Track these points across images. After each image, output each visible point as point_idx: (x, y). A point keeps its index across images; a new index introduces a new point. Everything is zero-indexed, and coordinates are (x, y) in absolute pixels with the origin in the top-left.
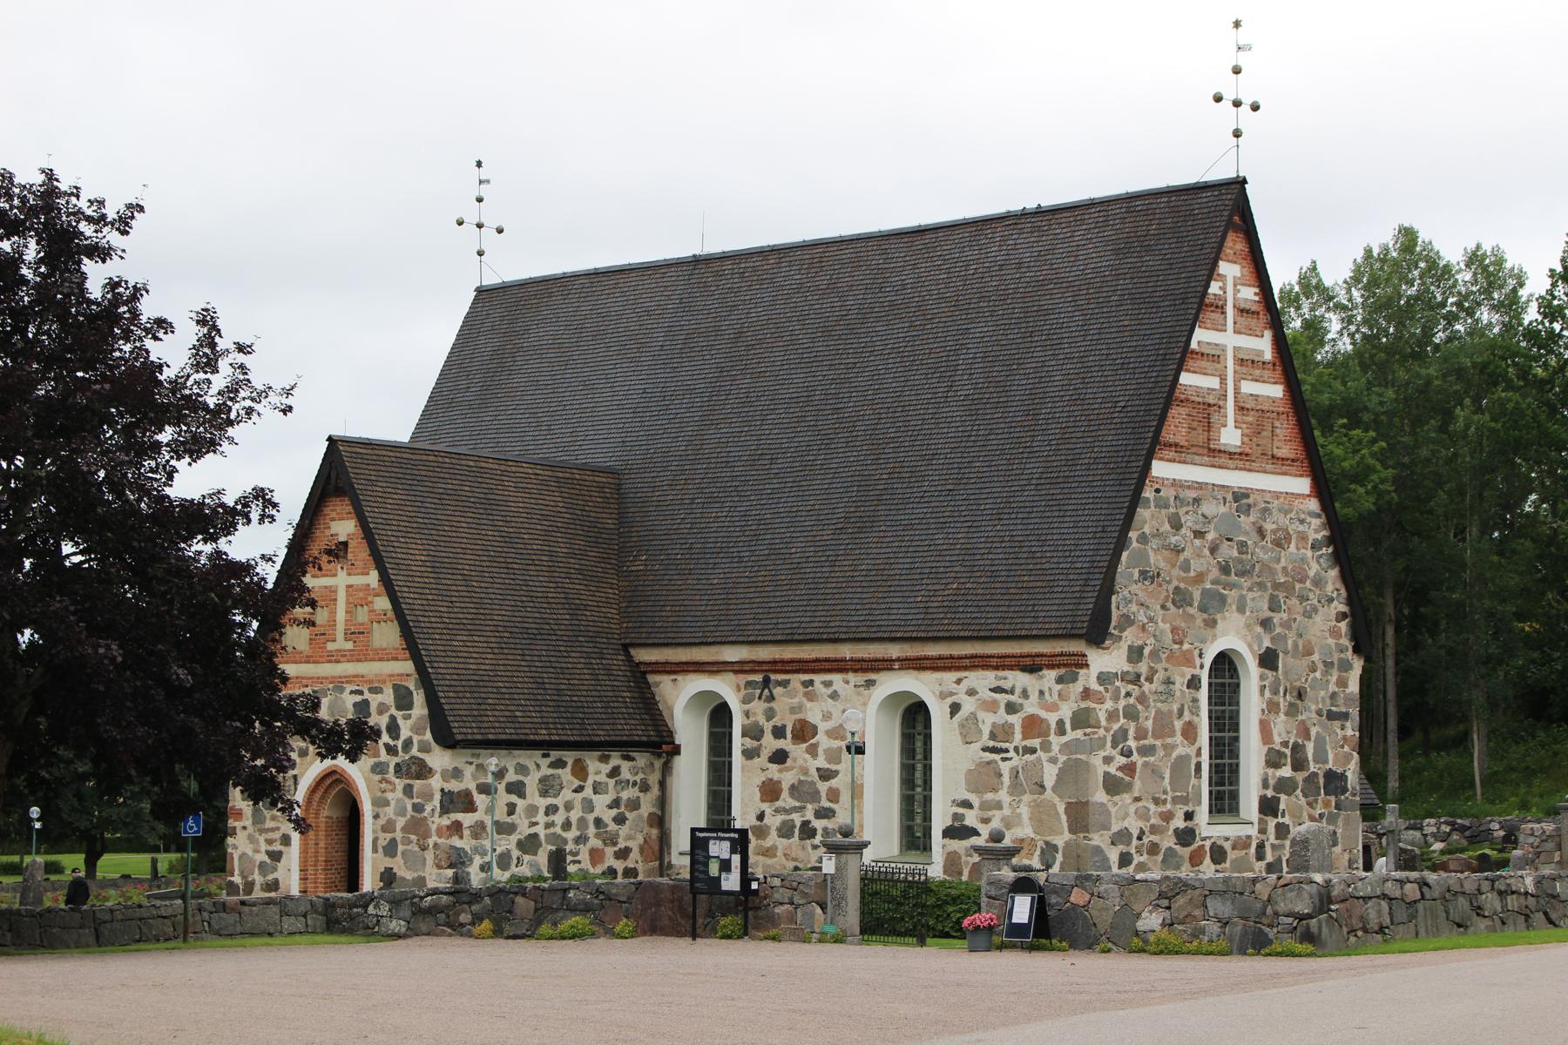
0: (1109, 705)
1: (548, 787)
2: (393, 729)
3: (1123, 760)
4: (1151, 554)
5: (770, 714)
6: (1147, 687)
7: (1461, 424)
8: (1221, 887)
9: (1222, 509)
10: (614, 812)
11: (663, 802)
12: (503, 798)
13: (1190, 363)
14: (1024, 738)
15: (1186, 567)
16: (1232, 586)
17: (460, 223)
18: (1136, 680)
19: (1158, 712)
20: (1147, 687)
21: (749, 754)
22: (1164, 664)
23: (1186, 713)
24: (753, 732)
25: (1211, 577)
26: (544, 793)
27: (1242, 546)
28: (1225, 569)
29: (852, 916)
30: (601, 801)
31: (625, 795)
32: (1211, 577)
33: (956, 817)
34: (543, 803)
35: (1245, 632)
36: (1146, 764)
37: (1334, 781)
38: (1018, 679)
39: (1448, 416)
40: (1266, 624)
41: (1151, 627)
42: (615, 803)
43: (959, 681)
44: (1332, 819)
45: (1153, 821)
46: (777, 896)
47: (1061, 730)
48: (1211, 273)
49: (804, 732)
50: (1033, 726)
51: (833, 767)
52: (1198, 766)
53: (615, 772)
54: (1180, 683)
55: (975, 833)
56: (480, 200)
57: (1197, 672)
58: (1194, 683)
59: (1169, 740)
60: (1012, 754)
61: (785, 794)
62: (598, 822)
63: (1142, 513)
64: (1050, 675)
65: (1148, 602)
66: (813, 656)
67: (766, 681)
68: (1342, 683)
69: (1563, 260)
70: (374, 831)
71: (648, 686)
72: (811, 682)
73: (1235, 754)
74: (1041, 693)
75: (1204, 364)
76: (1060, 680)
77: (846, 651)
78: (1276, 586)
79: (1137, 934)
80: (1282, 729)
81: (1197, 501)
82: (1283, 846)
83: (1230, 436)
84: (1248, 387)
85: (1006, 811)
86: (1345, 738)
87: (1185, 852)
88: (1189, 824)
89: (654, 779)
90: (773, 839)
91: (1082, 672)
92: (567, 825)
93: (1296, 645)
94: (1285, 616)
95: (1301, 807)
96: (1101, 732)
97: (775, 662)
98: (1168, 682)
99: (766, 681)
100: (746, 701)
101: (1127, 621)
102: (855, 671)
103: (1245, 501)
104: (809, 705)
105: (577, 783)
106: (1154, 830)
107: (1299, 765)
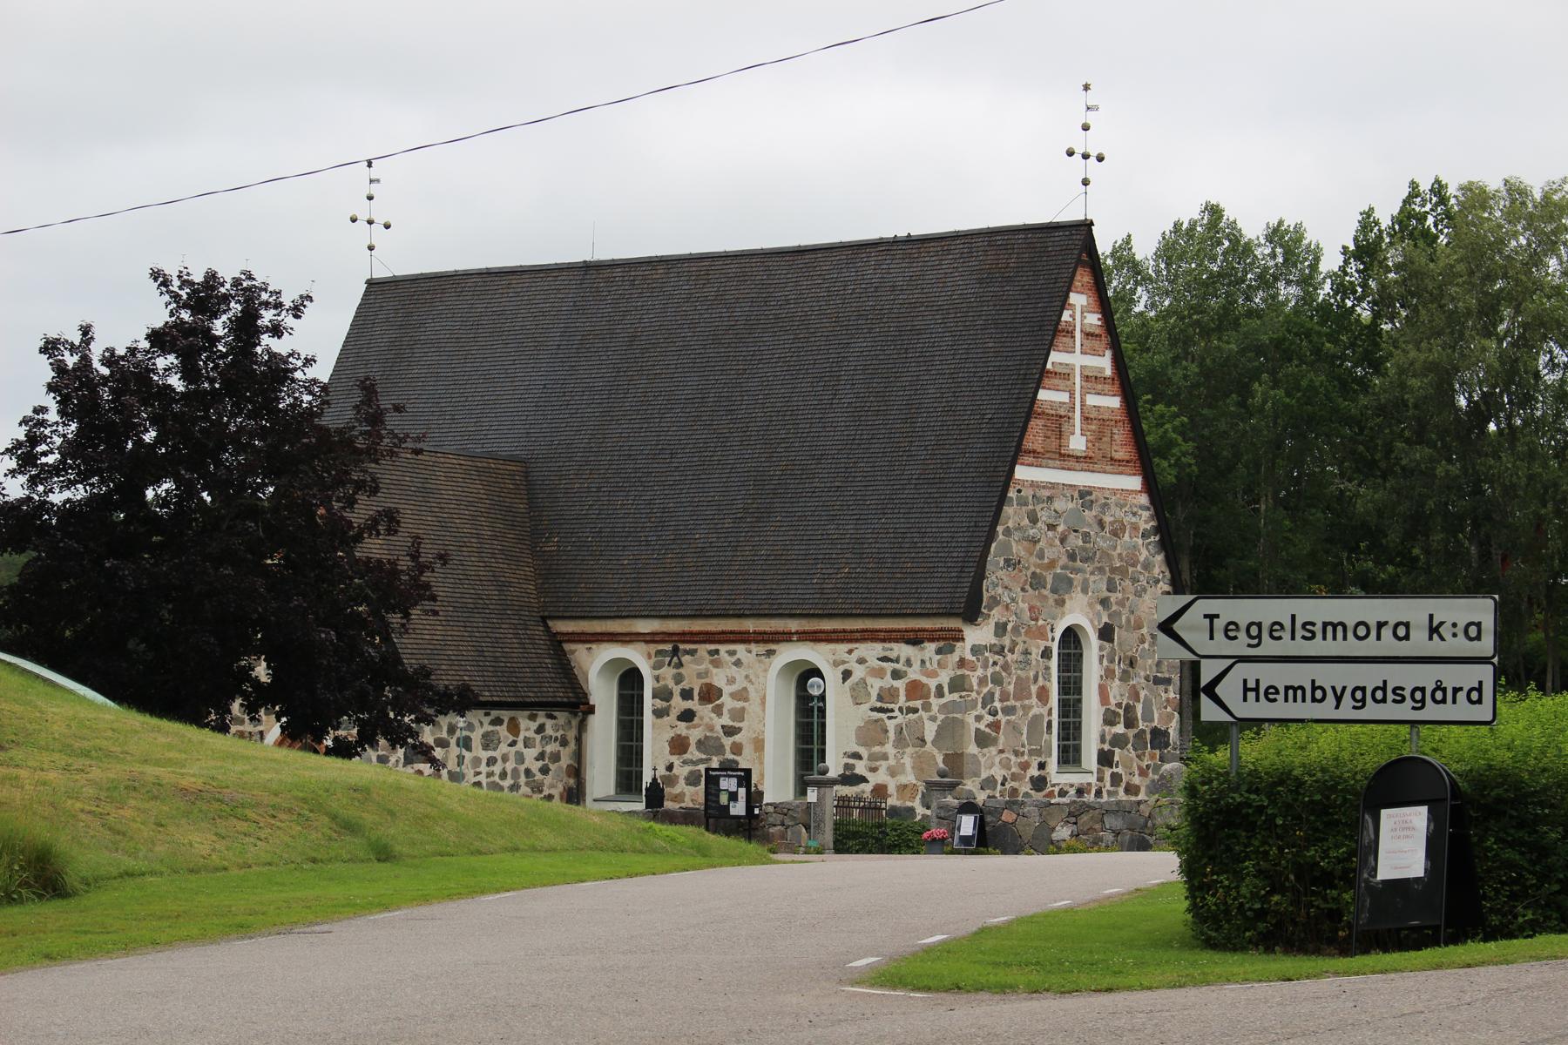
0: (980, 672)
1: (489, 742)
3: (991, 719)
5: (678, 679)
6: (1009, 657)
7: (1258, 399)
8: (1115, 808)
9: (1071, 505)
10: (540, 763)
11: (579, 755)
12: (454, 751)
13: (1046, 381)
14: (908, 699)
15: (1041, 556)
16: (1076, 571)
17: (354, 220)
18: (1000, 651)
19: (1018, 678)
20: (1009, 657)
21: (659, 714)
22: (1023, 638)
24: (663, 694)
25: (1061, 563)
26: (486, 747)
27: (1086, 536)
28: (1072, 556)
29: (828, 836)
30: (531, 754)
31: (549, 749)
32: (1061, 563)
33: (847, 766)
34: (485, 755)
36: (1008, 722)
38: (902, 650)
39: (1245, 391)
40: (1104, 602)
41: (1013, 607)
42: (541, 756)
43: (850, 652)
46: (771, 820)
47: (940, 692)
48: (1064, 304)
49: (710, 694)
50: (915, 690)
51: (737, 725)
53: (541, 729)
55: (864, 780)
56: (370, 198)
57: (1049, 644)
58: (1046, 654)
60: (897, 713)
61: (693, 748)
62: (528, 772)
63: (1008, 510)
64: (931, 647)
65: (1011, 585)
66: (720, 628)
67: (675, 651)
69: (1356, 239)
71: (564, 653)
72: (717, 652)
73: (1078, 714)
74: (923, 662)
75: (1056, 381)
76: (939, 651)
77: (750, 625)
78: (1113, 570)
79: (1052, 842)
81: (1050, 499)
82: (1116, 793)
83: (1077, 443)
84: (1092, 400)
85: (892, 762)
86: (1168, 700)
88: (1042, 773)
89: (571, 734)
90: (681, 787)
91: (959, 644)
92: (503, 775)
93: (1128, 620)
94: (1120, 595)
96: (974, 695)
97: (683, 634)
98: (1026, 653)
99: (675, 651)
100: (657, 666)
101: (995, 601)
102: (757, 642)
104: (715, 671)
105: (511, 738)
106: (1014, 777)
107: (1130, 723)
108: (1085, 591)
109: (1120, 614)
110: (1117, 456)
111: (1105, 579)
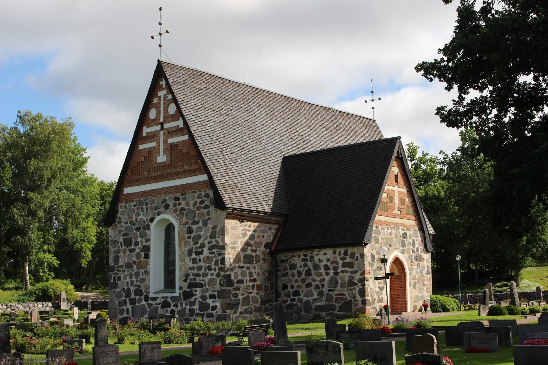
2: (413, 244)
70: (410, 280)
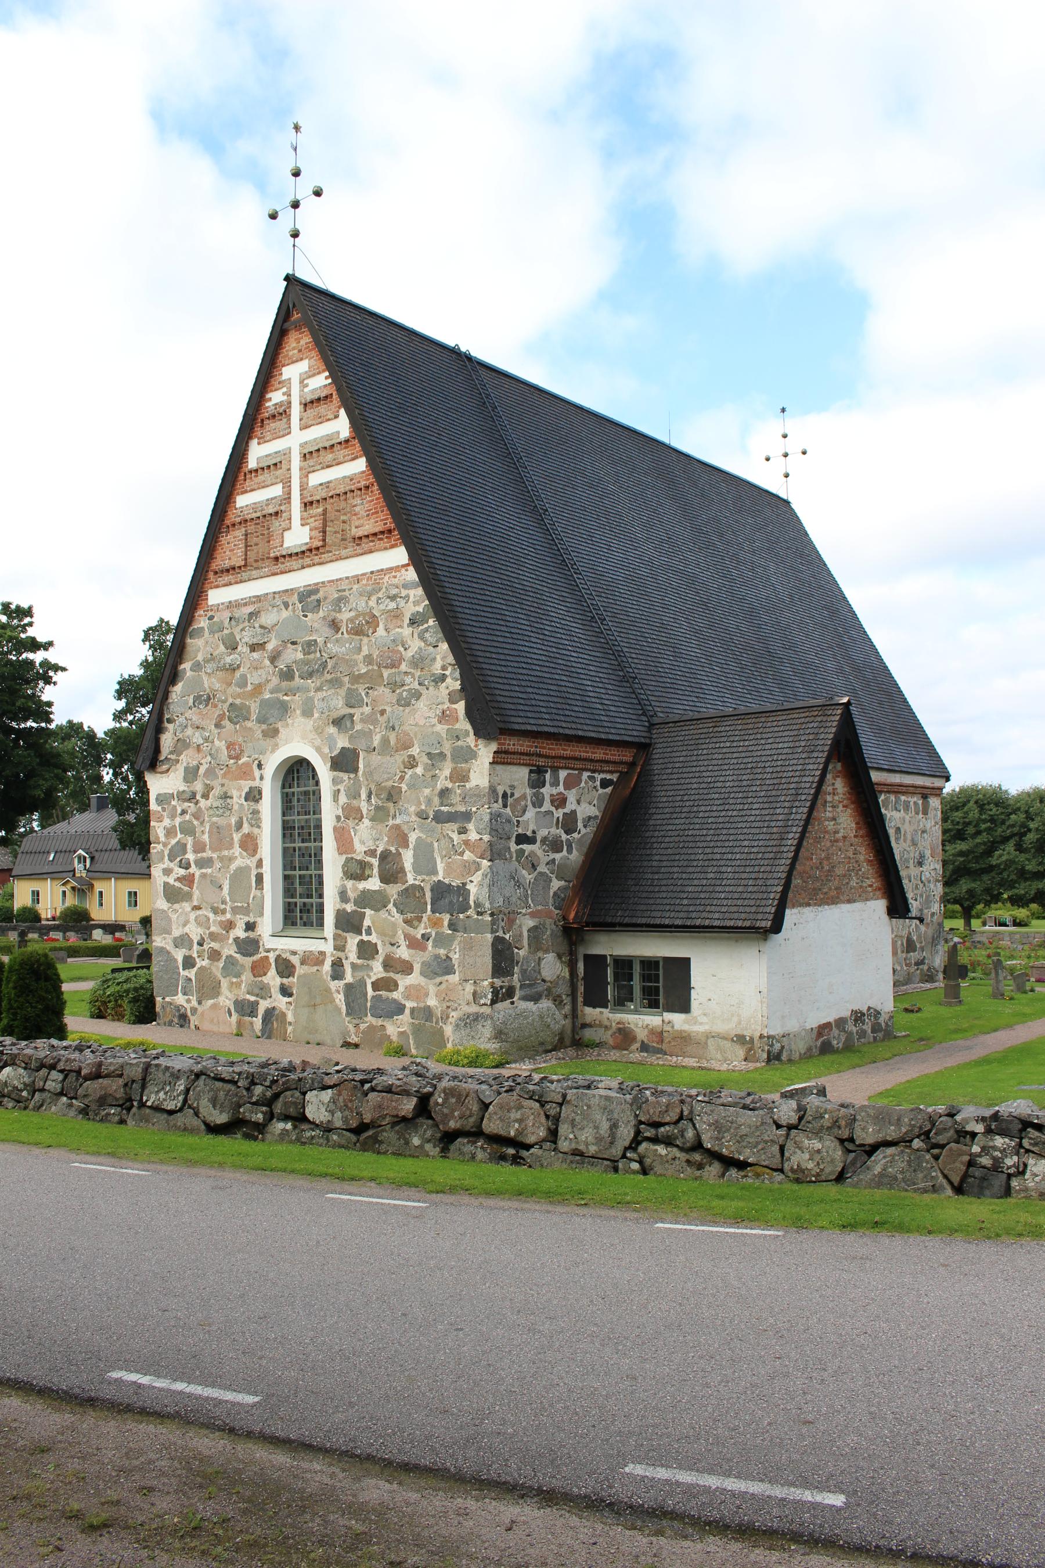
0: (167, 822)
4: (205, 678)
6: (203, 803)
9: (285, 614)
15: (243, 682)
18: (192, 797)
20: (203, 803)
23: (246, 825)
25: (270, 686)
28: (287, 675)
32: (270, 686)
35: (313, 735)
36: (204, 876)
37: (449, 897)
40: (338, 722)
44: (441, 941)
45: (213, 929)
52: (260, 878)
54: (238, 799)
56: (785, 436)
57: (257, 783)
59: (226, 853)
65: (203, 724)
68: (460, 777)
75: (261, 478)
78: (356, 679)
80: (366, 837)
82: (370, 968)
86: (466, 843)
87: (248, 961)
88: (251, 934)
93: (385, 741)
94: (367, 710)
95: (394, 925)
98: (226, 796)
101: (182, 745)
103: (313, 597)
107: (391, 874)
108: (307, 713)
109: (369, 734)
110: (360, 533)
111: (342, 692)
